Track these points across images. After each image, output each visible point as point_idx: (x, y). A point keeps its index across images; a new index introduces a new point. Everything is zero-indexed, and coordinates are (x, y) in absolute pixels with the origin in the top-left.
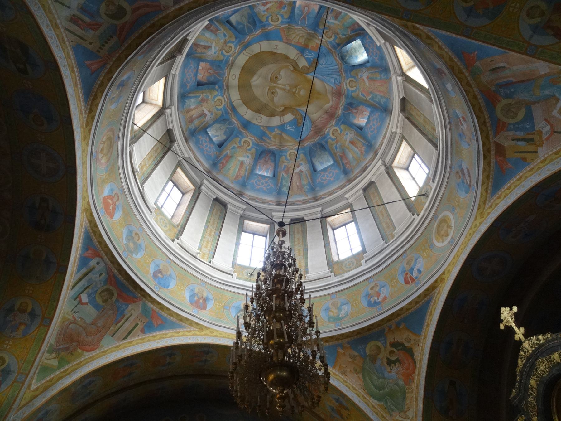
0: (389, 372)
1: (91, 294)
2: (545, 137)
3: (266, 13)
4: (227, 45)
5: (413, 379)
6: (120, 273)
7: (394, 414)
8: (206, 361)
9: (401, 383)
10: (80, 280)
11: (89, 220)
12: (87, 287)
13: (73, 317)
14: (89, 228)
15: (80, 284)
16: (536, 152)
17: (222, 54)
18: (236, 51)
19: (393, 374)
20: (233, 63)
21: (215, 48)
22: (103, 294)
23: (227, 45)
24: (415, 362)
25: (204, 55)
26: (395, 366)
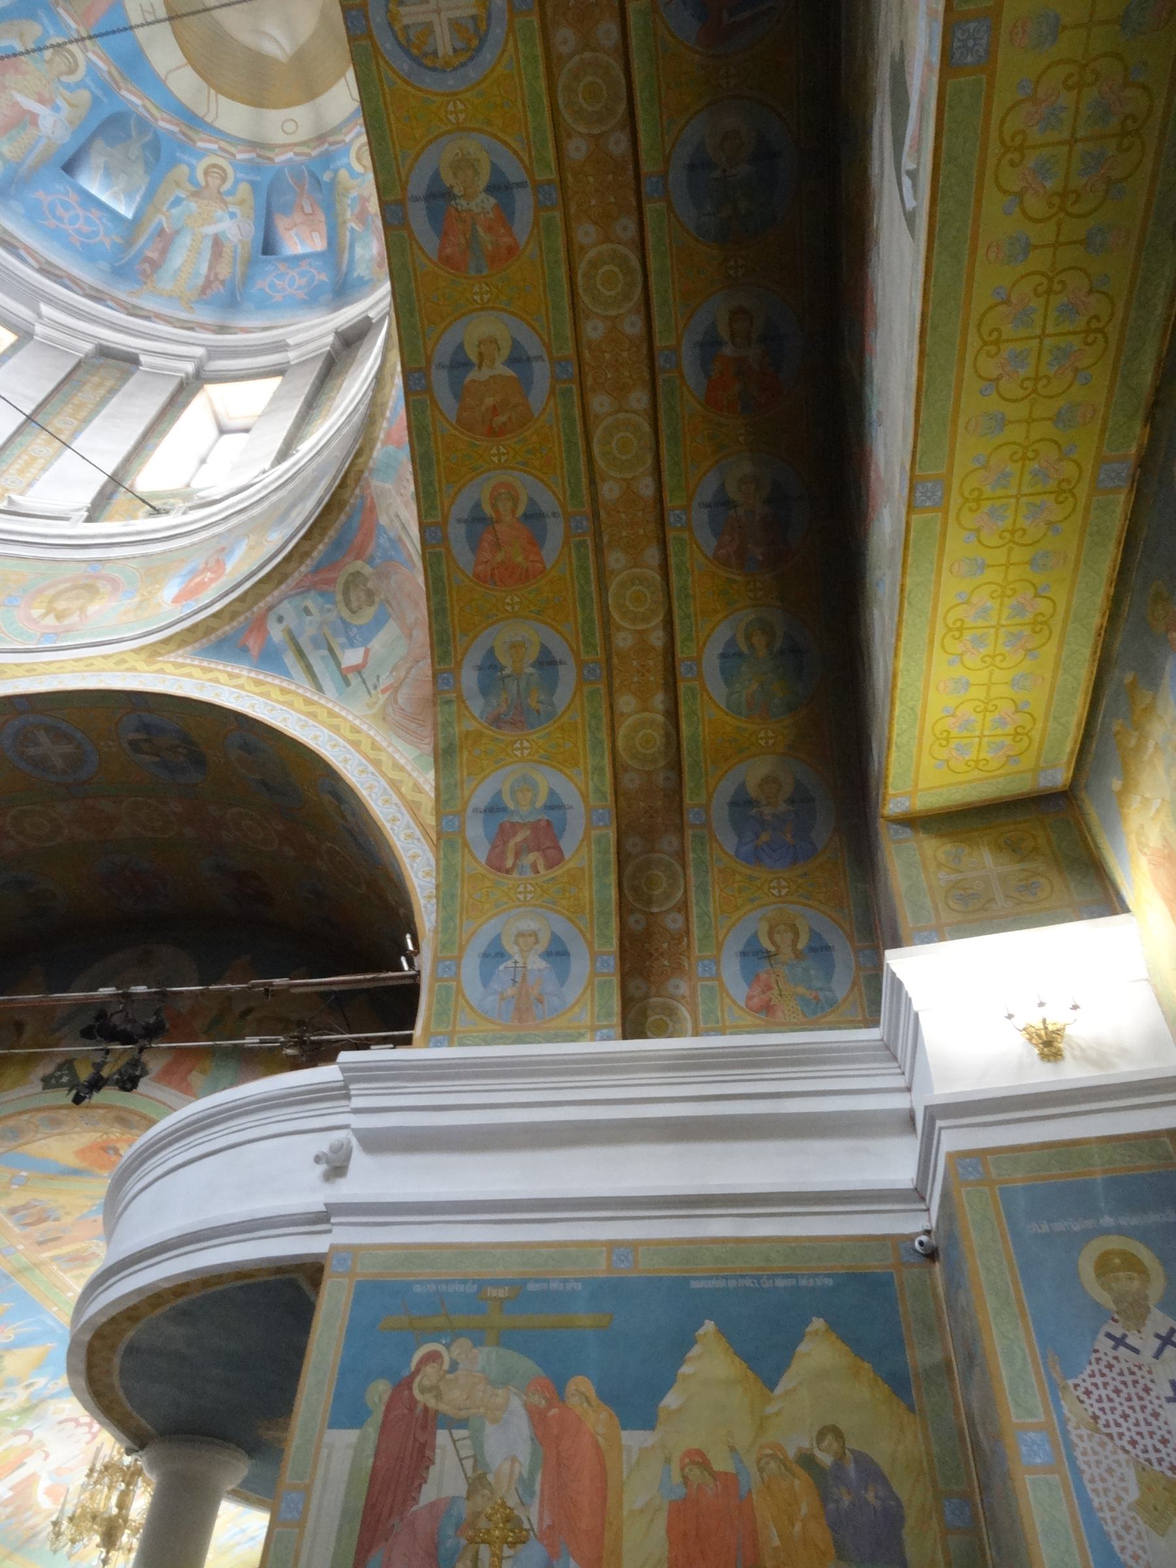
1: (348, 637)
3: (60, 102)
4: (203, 183)
6: (307, 554)
8: (499, 187)
10: (309, 669)
11: (180, 646)
12: (331, 650)
13: (383, 691)
14: (197, 645)
15: (318, 667)
17: (231, 192)
18: (214, 146)
20: (253, 145)
21: (220, 220)
22: (354, 605)
23: (203, 183)
25: (239, 250)
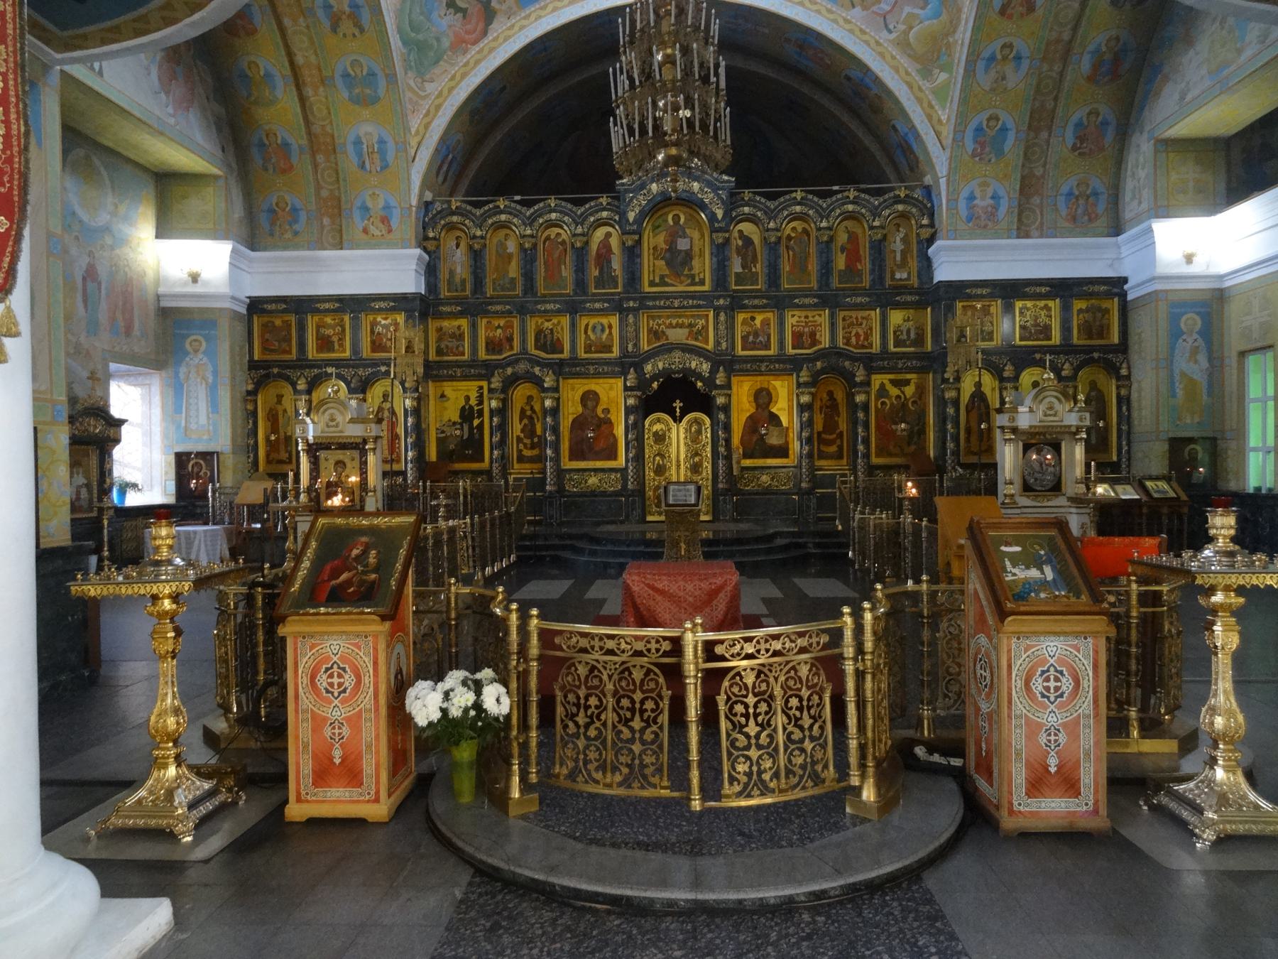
0: (440, 16)
2: (875, 8)
5: (465, 52)
7: (410, 74)
9: (446, 43)
16: (854, 6)
19: (445, 22)
24: (485, 33)
26: (455, 14)
